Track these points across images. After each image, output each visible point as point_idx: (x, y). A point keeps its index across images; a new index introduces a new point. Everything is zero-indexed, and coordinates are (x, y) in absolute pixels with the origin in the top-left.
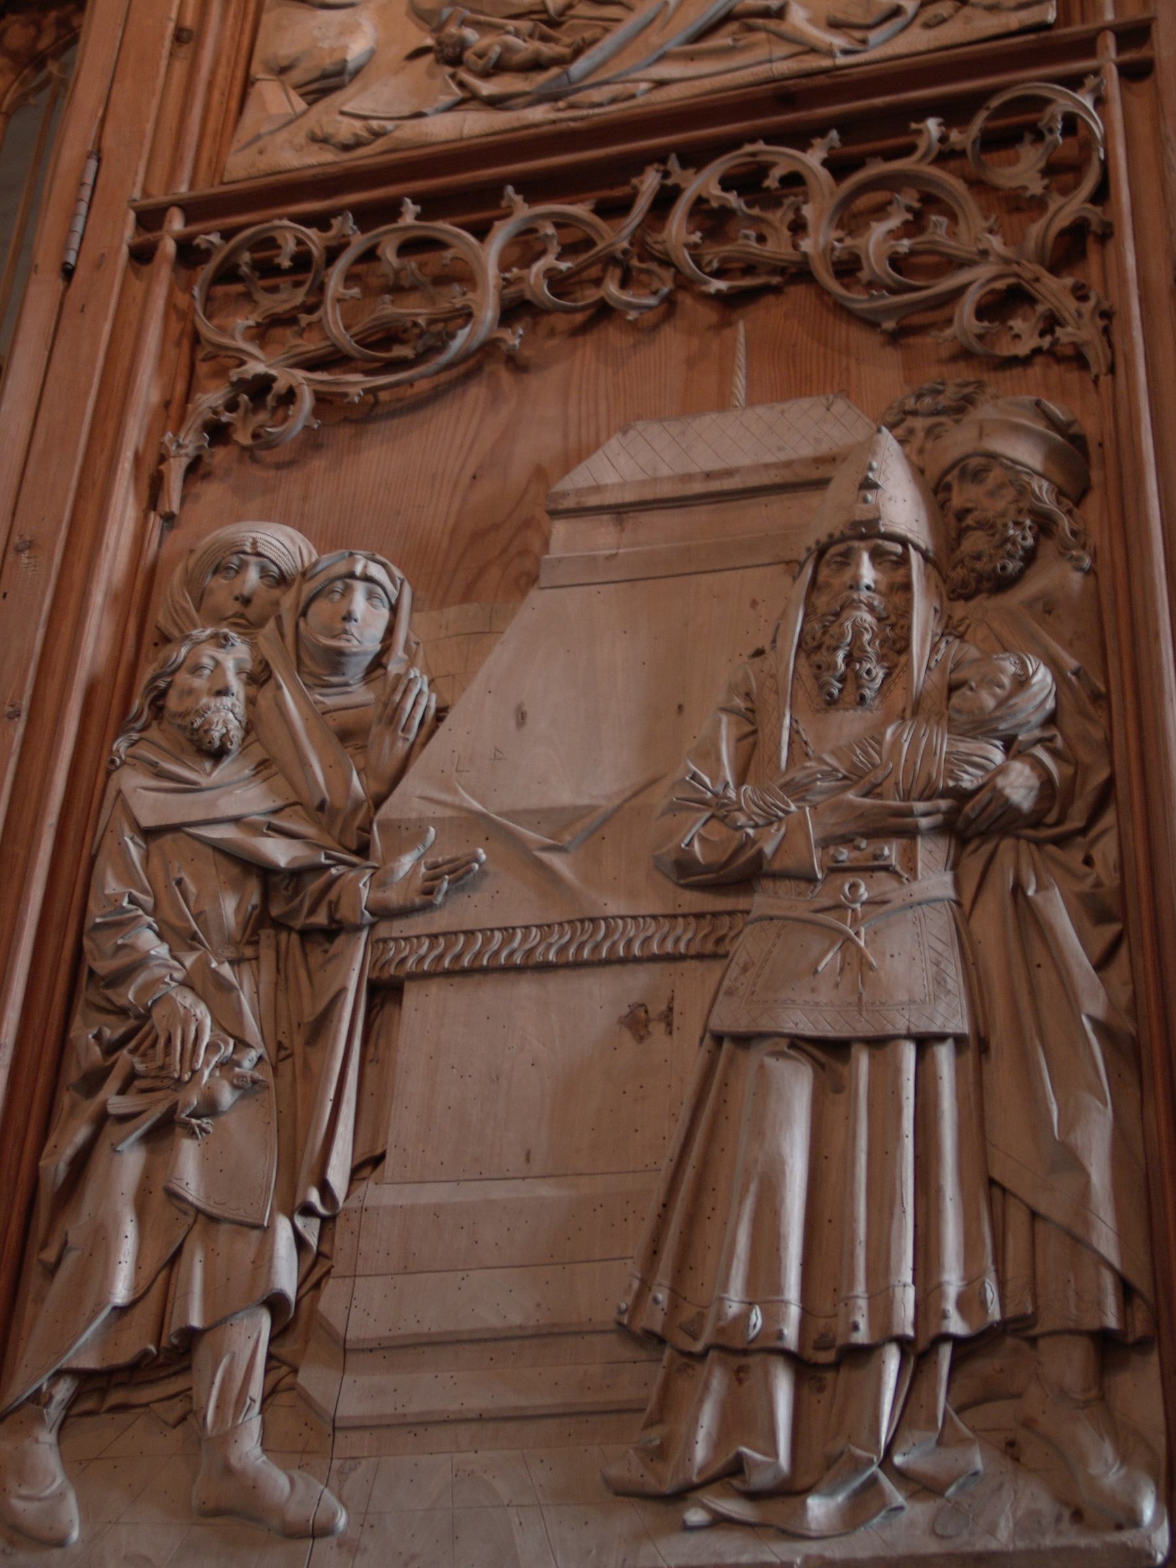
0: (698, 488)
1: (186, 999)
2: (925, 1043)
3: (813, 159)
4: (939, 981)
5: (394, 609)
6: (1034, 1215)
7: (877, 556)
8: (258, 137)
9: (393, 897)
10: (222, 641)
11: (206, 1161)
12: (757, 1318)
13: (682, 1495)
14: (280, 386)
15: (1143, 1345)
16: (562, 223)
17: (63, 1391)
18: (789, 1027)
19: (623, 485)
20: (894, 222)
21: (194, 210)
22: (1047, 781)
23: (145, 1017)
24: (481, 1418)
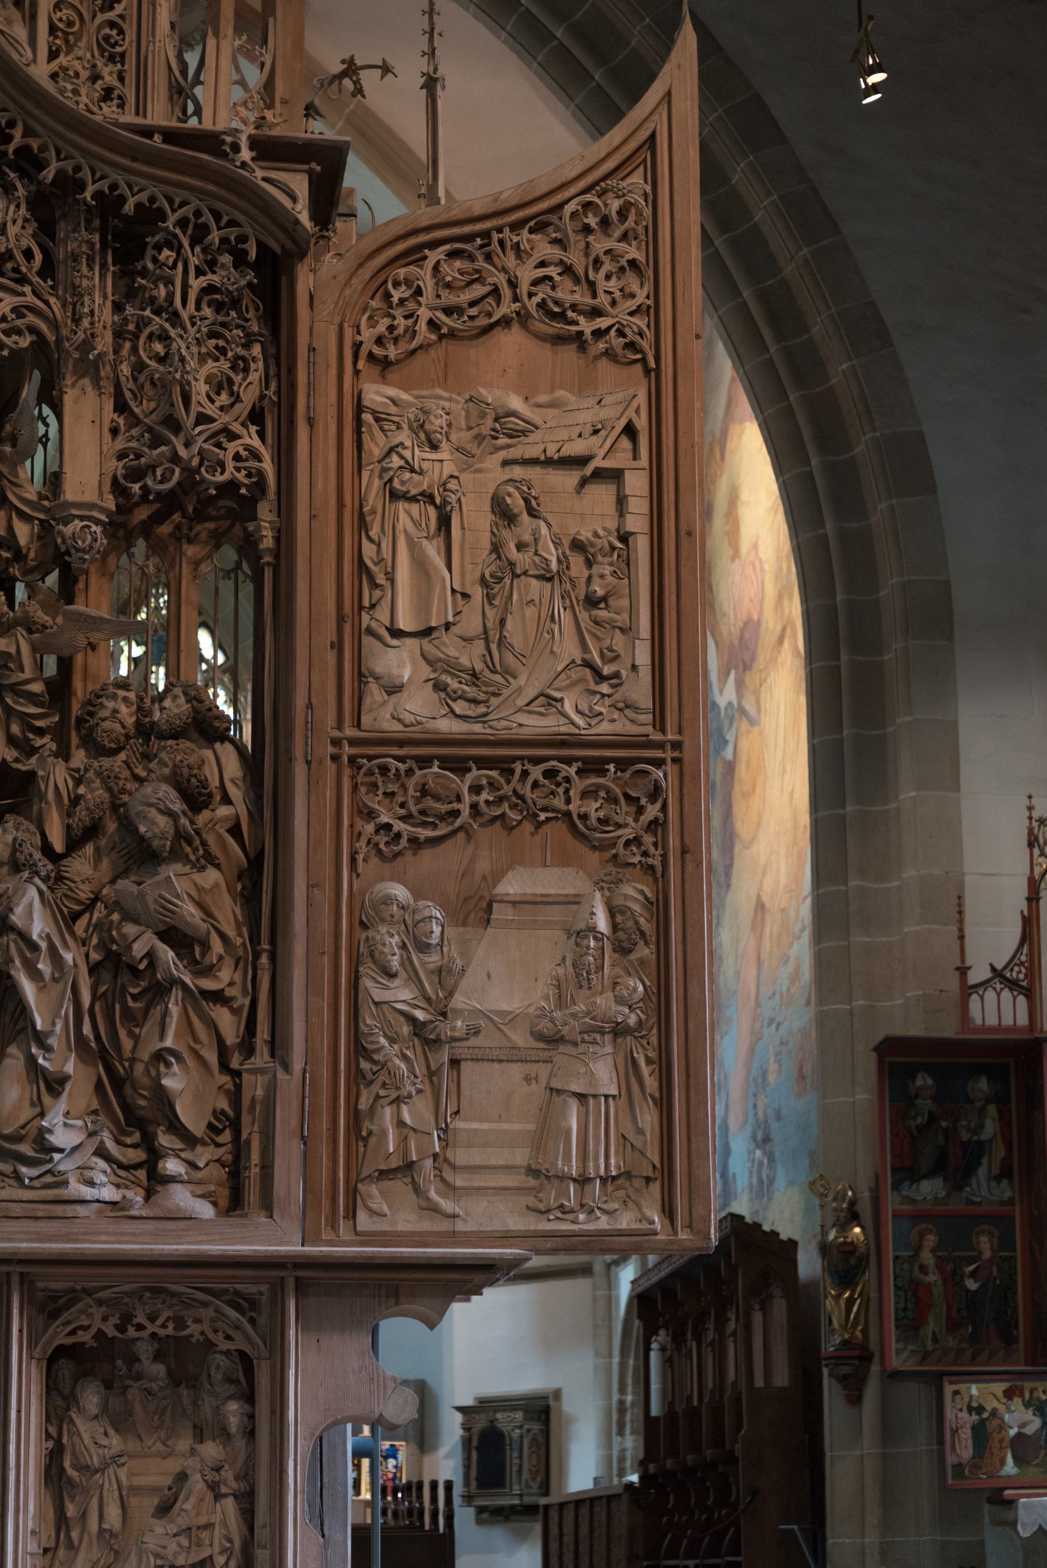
0: (539, 899)
1: (397, 1061)
2: (606, 1097)
3: (572, 770)
4: (611, 1079)
5: (443, 927)
6: (632, 1145)
7: (595, 938)
8: (371, 710)
9: (457, 1034)
10: (392, 936)
11: (410, 1111)
12: (566, 1169)
13: (548, 1211)
14: (395, 829)
15: (656, 1179)
16: (488, 777)
17: (376, 1174)
18: (572, 1090)
19: (516, 894)
20: (598, 805)
21: (353, 742)
22: (640, 1021)
23: (384, 1065)
24: (494, 1188)
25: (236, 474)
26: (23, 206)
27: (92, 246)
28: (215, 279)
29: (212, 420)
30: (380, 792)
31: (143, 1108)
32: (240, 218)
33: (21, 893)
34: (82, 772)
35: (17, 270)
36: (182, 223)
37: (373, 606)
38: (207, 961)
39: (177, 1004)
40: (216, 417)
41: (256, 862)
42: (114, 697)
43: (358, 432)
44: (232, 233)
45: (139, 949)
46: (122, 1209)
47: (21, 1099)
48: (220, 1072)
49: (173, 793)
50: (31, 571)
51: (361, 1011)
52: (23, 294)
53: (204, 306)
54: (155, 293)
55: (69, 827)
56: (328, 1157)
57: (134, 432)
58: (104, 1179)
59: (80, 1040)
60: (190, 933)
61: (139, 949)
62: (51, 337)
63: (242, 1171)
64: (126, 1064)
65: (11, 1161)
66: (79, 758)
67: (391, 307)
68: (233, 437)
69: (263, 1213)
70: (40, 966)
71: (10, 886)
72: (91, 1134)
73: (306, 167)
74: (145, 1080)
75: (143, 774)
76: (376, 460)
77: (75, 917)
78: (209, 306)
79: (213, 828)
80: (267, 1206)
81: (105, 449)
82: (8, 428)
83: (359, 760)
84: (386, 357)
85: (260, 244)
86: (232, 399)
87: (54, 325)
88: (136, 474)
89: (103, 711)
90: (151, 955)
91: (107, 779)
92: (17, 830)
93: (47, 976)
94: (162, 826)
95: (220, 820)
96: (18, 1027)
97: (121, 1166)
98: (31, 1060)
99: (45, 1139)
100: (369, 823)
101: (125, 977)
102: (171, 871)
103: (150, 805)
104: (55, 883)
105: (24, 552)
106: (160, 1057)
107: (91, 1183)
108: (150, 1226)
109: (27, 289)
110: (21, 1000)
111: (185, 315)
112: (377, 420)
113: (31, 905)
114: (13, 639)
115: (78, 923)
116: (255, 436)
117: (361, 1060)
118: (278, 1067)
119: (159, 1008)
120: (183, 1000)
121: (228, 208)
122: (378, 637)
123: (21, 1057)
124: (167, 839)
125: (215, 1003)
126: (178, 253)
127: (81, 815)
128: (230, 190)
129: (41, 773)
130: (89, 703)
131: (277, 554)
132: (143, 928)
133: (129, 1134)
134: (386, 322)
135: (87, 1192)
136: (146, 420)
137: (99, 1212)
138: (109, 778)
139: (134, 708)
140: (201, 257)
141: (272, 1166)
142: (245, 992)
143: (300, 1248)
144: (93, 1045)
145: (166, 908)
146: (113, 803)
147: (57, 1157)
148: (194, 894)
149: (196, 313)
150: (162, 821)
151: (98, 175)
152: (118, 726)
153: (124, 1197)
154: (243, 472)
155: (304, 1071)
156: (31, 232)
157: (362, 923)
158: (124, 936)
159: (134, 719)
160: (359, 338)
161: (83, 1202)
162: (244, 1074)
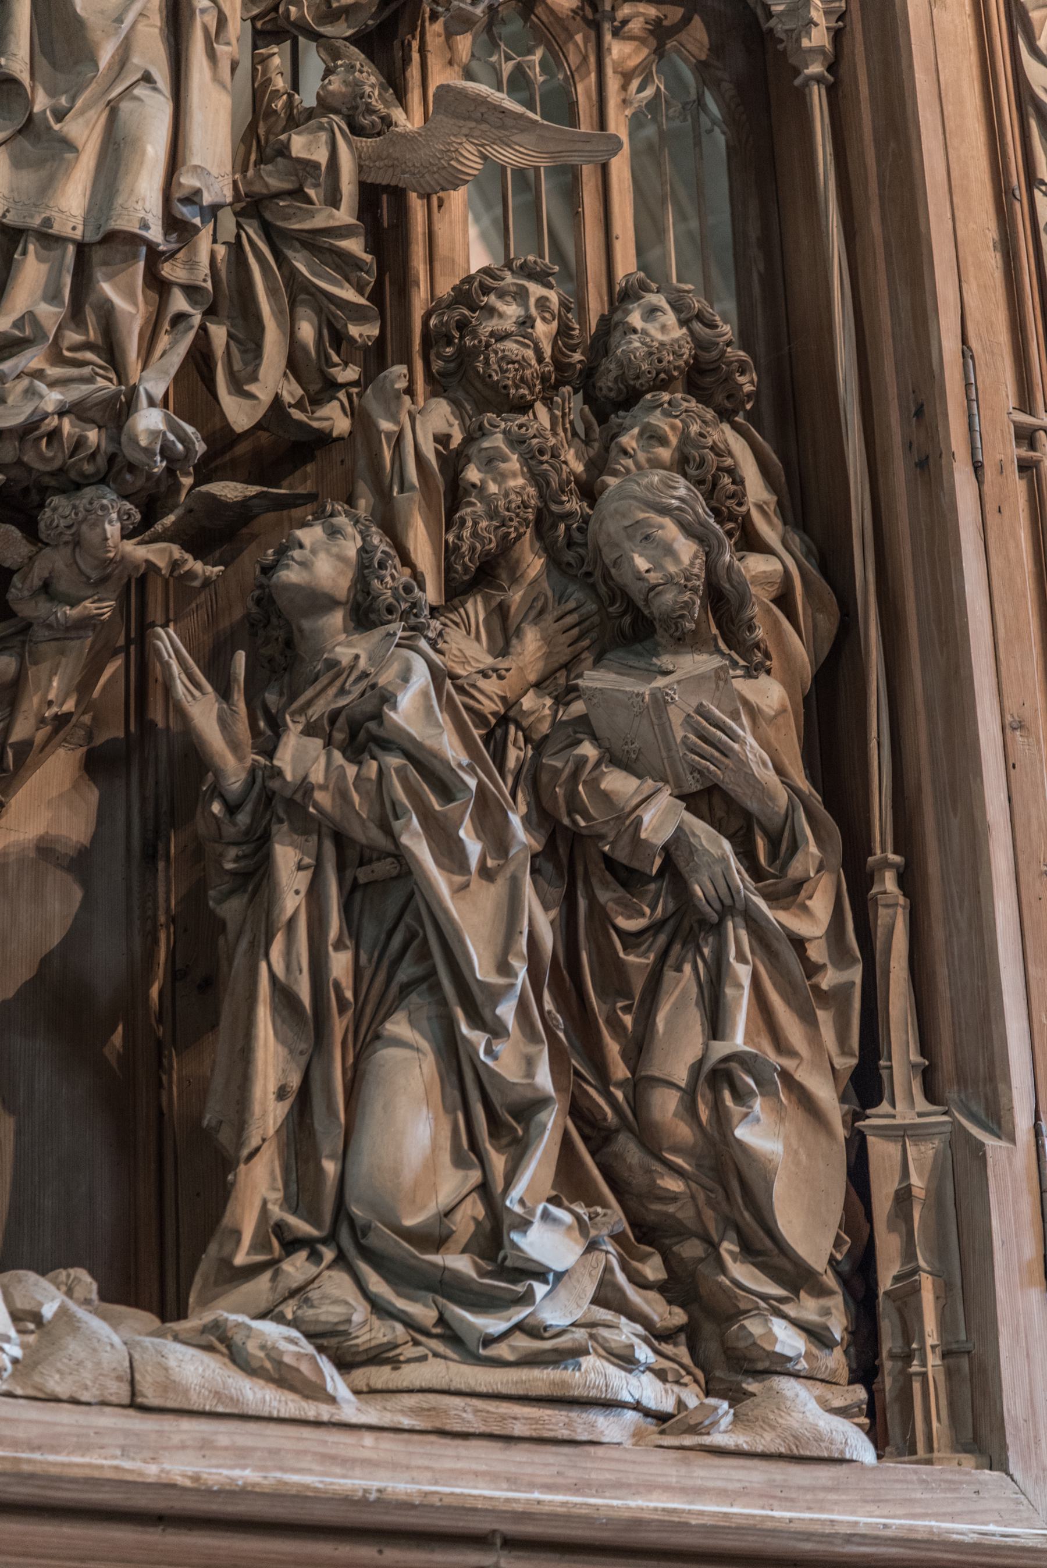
39: (741, 958)
60: (752, 806)
70: (462, 833)
93: (474, 862)
94: (686, 559)
96: (404, 974)
119: (687, 968)
124: (694, 590)
132: (650, 784)
138: (542, 452)
139: (555, 324)
146: (540, 513)
150: (686, 549)
152: (530, 353)
158: (606, 798)
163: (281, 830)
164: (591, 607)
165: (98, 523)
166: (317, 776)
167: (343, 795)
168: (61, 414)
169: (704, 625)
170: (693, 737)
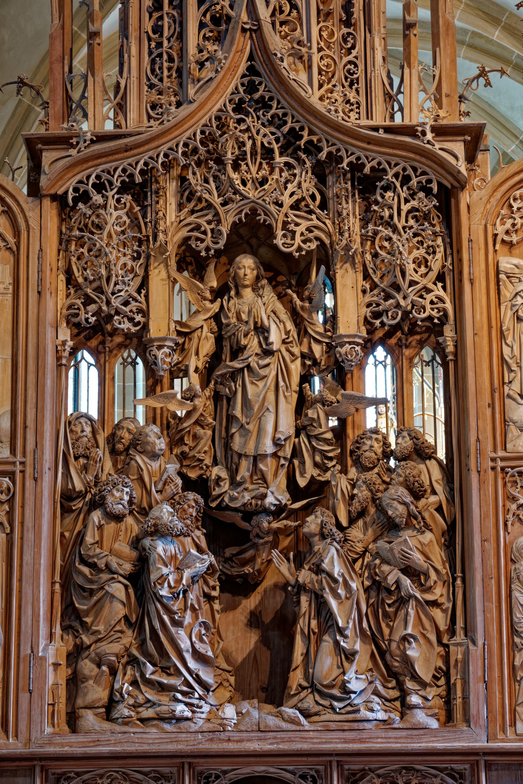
21: (503, 459)
25: (432, 312)
26: (310, 172)
27: (347, 190)
28: (414, 203)
29: (417, 283)
30: (519, 486)
31: (397, 667)
32: (428, 170)
33: (327, 551)
34: (355, 481)
35: (307, 206)
36: (396, 175)
37: (510, 382)
38: (428, 584)
40: (420, 281)
41: (451, 527)
42: (371, 438)
43: (498, 285)
44: (423, 179)
45: (391, 579)
46: (389, 724)
47: (332, 664)
48: (438, 646)
49: (406, 492)
50: (323, 371)
51: (514, 610)
52: (311, 220)
53: (410, 219)
54: (383, 214)
55: (349, 512)
56: (499, 692)
57: (375, 292)
58: (379, 708)
59: (362, 631)
61: (391, 579)
62: (327, 241)
63: (452, 701)
64: (387, 643)
65: (328, 699)
66: (353, 472)
67: (512, 213)
68: (429, 291)
69: (465, 724)
70: (339, 591)
71: (321, 547)
72: (371, 683)
73: (462, 138)
74: (398, 652)
75: (388, 480)
76: (508, 299)
77: (355, 561)
78: (412, 219)
79: (427, 509)
80: (467, 721)
81: (359, 303)
82: (307, 293)
83: (507, 469)
84: (512, 241)
85: (439, 184)
86: (428, 270)
87: (329, 235)
88: (377, 315)
89: (365, 446)
90: (398, 583)
91: (369, 485)
92: (323, 516)
93: (343, 597)
95: (431, 504)
96: (328, 625)
97: (387, 700)
98: (337, 643)
99: (346, 686)
100: (513, 503)
101: (383, 595)
102: (407, 534)
103: (394, 500)
104: (344, 543)
105: (319, 361)
106: (405, 639)
107: (372, 710)
108: (404, 733)
109: (314, 217)
110: (329, 609)
111: (400, 226)
112: (508, 277)
113: (332, 558)
114: (316, 410)
115: (356, 564)
116: (441, 289)
117: (515, 637)
118: (469, 642)
119: (403, 611)
120: (416, 606)
121: (421, 165)
122: (514, 400)
123: (331, 641)
124: (403, 517)
125: (433, 607)
126: (394, 192)
127: (356, 506)
128: (420, 155)
129: (333, 483)
130: (357, 442)
131: (456, 354)
132: (392, 567)
133: (390, 682)
134: (511, 221)
135: (370, 715)
136: (381, 285)
137: (377, 726)
139: (381, 443)
140: (407, 192)
141: (469, 698)
142: (449, 599)
143: (486, 744)
144: (369, 633)
145: (405, 556)
146: (373, 498)
147: (353, 696)
148: (419, 547)
149: (406, 224)
150: (401, 508)
151: (349, 153)
153: (389, 717)
154: (436, 310)
155: (484, 644)
156: (314, 184)
157: (512, 560)
158: (382, 572)
159: (381, 449)
160: (496, 232)
161: (368, 721)
162: (451, 646)
163: (302, 592)
164: (385, 520)
165: (261, 524)
166: (308, 580)
167: (314, 584)
168: (252, 499)
169: (410, 523)
170: (401, 556)
